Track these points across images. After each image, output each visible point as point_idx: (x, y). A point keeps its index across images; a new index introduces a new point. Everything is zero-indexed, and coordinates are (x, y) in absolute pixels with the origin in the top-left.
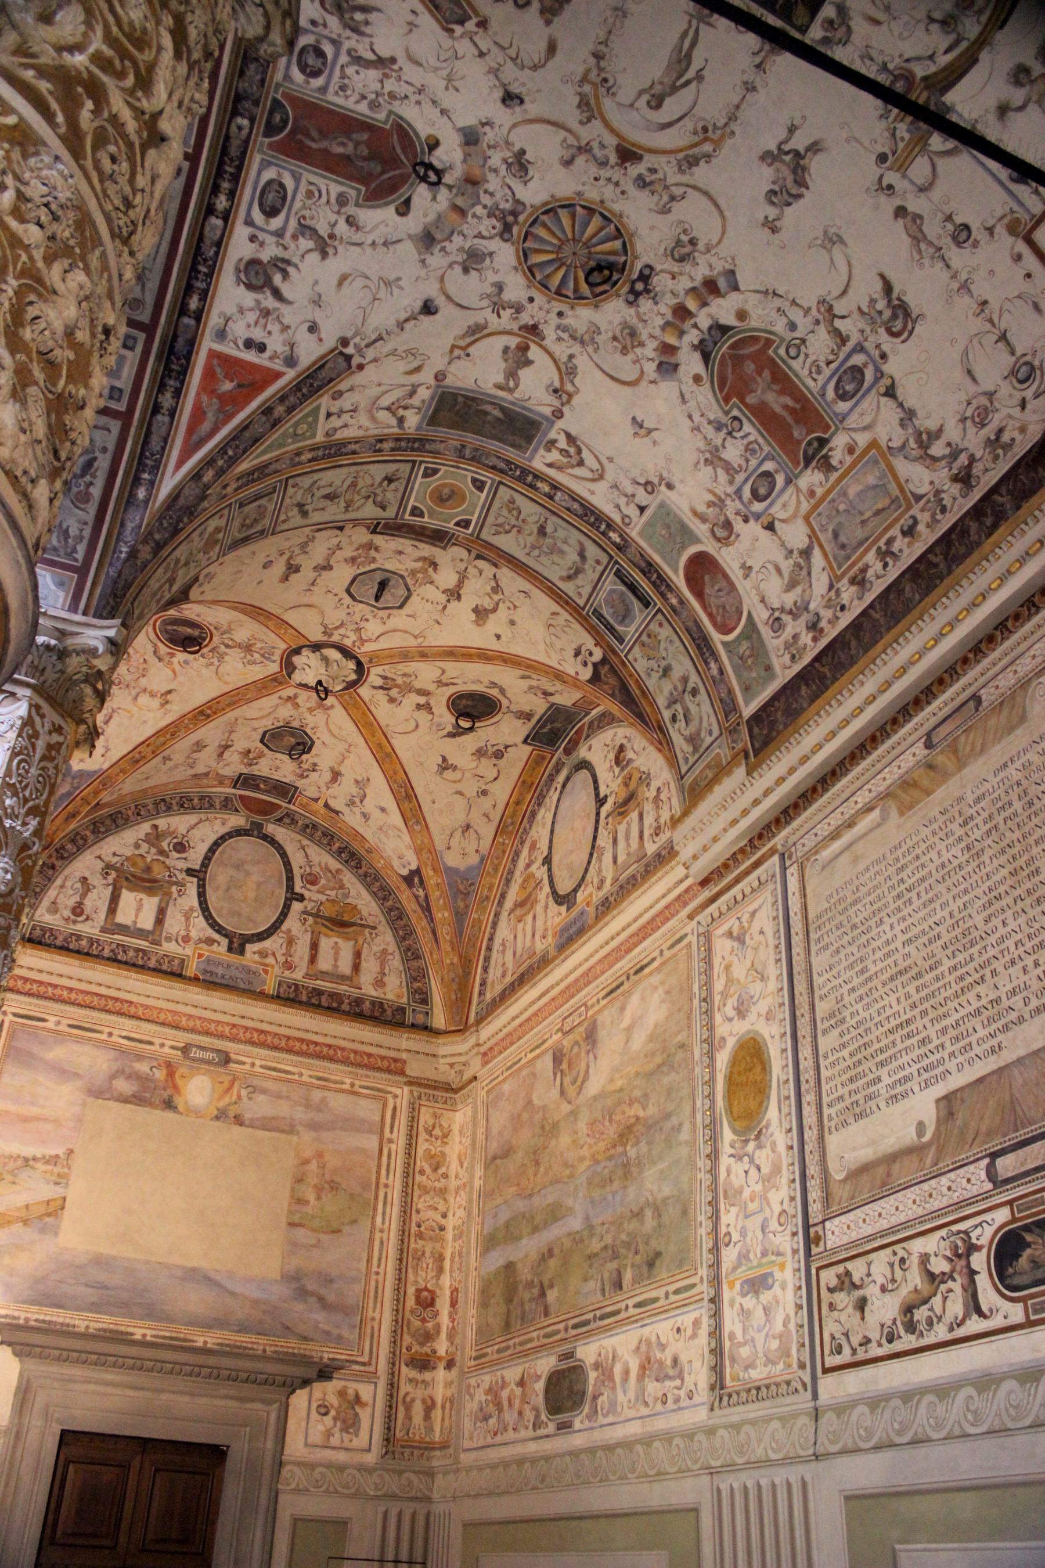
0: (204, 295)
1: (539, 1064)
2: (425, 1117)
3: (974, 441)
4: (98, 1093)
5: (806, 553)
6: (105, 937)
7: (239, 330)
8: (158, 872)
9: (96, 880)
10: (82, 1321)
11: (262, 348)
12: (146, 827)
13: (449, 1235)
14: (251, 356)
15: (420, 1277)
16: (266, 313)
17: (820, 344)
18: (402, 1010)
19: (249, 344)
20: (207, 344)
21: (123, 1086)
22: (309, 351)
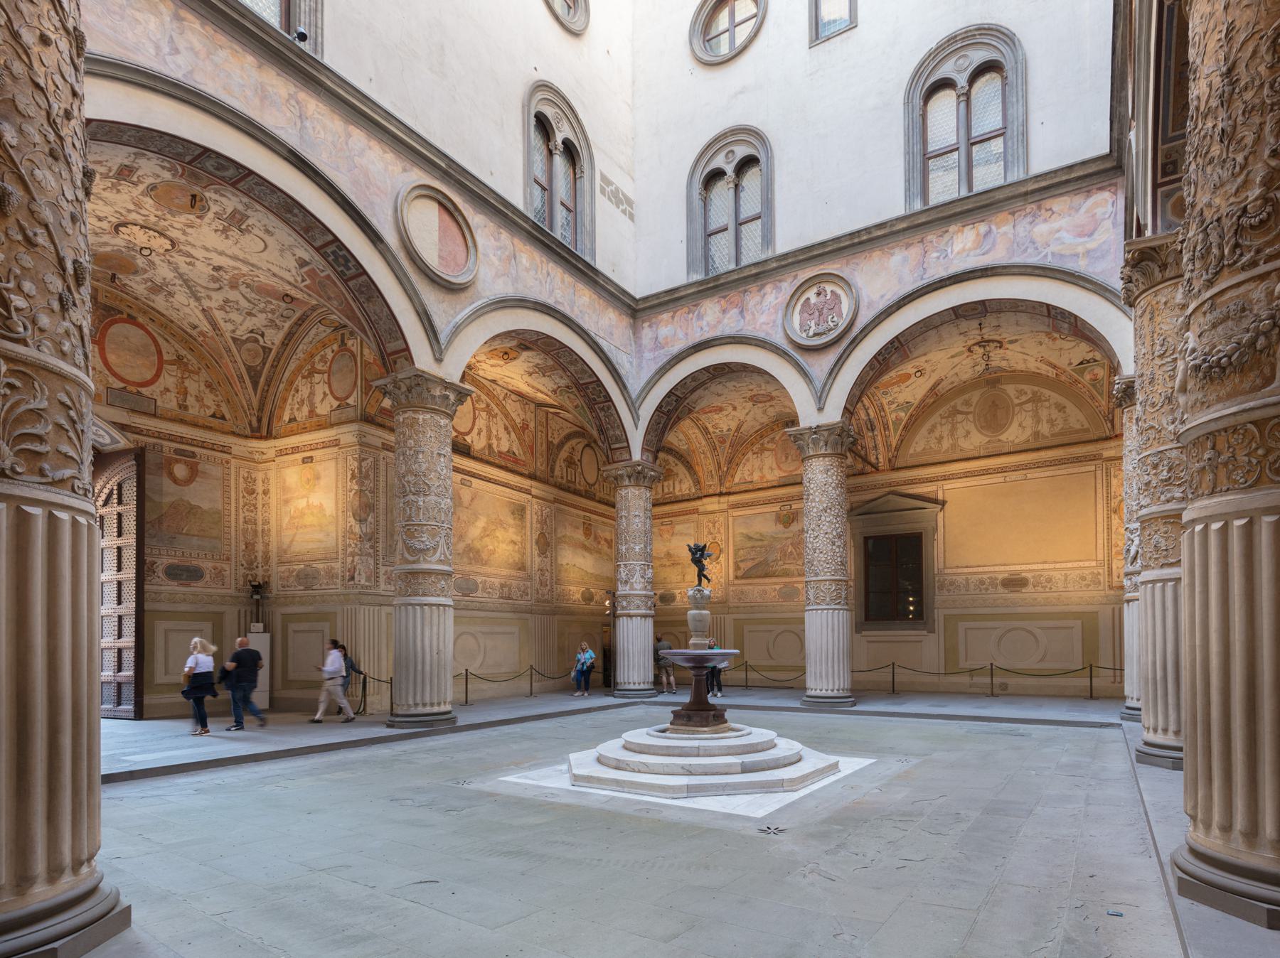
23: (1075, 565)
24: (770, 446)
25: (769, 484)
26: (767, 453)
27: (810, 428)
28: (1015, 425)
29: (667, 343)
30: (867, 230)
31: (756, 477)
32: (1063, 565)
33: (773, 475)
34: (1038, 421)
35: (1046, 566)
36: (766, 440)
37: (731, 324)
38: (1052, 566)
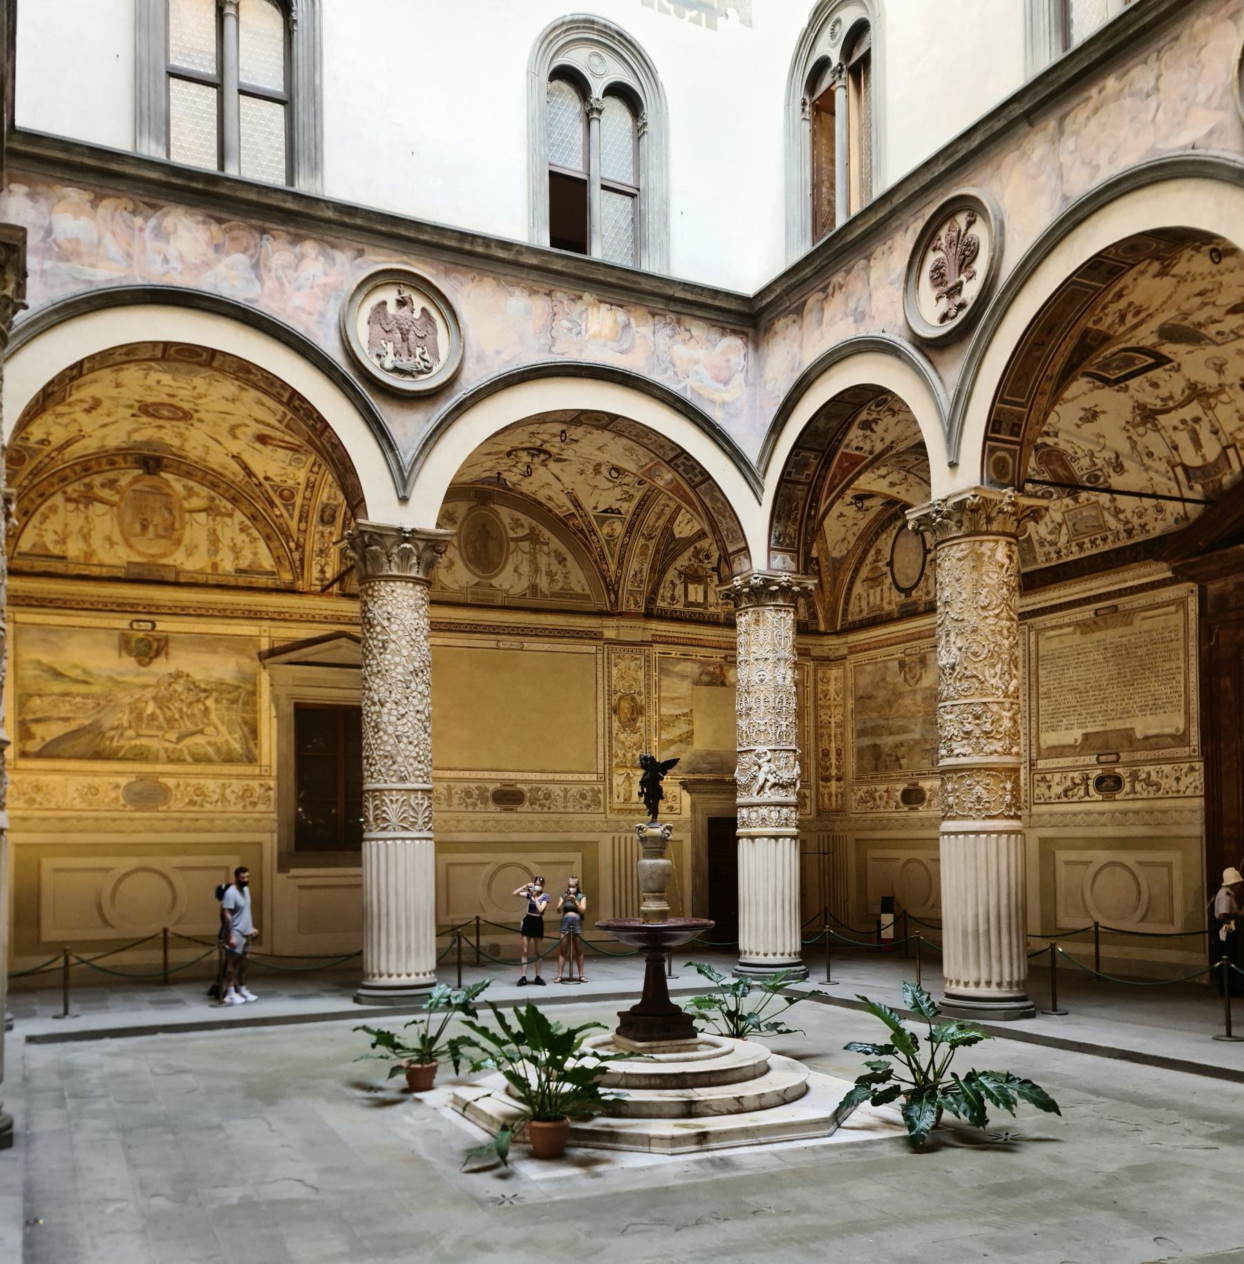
0: (845, 434)
1: (889, 664)
2: (820, 674)
3: (1136, 521)
4: (697, 683)
5: (1060, 525)
6: (686, 609)
7: (854, 444)
8: (701, 572)
9: (677, 581)
10: (707, 777)
11: (861, 449)
12: (692, 549)
13: (833, 725)
14: (857, 453)
15: (824, 744)
16: (866, 437)
17: (1085, 462)
18: (806, 624)
19: (858, 448)
20: (842, 450)
21: (705, 678)
22: (879, 447)
23: (576, 777)
24: (106, 494)
25: (105, 572)
26: (98, 508)
27: (401, 530)
28: (509, 569)
29: (78, 254)
30: (487, 241)
31: (74, 549)
32: (563, 777)
33: (118, 556)
34: (536, 571)
35: (545, 777)
36: (98, 480)
37: (228, 276)
38: (550, 777)
